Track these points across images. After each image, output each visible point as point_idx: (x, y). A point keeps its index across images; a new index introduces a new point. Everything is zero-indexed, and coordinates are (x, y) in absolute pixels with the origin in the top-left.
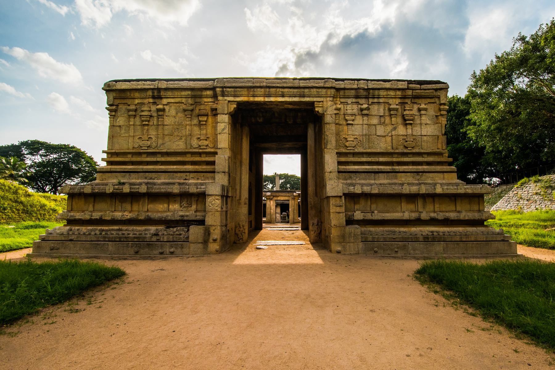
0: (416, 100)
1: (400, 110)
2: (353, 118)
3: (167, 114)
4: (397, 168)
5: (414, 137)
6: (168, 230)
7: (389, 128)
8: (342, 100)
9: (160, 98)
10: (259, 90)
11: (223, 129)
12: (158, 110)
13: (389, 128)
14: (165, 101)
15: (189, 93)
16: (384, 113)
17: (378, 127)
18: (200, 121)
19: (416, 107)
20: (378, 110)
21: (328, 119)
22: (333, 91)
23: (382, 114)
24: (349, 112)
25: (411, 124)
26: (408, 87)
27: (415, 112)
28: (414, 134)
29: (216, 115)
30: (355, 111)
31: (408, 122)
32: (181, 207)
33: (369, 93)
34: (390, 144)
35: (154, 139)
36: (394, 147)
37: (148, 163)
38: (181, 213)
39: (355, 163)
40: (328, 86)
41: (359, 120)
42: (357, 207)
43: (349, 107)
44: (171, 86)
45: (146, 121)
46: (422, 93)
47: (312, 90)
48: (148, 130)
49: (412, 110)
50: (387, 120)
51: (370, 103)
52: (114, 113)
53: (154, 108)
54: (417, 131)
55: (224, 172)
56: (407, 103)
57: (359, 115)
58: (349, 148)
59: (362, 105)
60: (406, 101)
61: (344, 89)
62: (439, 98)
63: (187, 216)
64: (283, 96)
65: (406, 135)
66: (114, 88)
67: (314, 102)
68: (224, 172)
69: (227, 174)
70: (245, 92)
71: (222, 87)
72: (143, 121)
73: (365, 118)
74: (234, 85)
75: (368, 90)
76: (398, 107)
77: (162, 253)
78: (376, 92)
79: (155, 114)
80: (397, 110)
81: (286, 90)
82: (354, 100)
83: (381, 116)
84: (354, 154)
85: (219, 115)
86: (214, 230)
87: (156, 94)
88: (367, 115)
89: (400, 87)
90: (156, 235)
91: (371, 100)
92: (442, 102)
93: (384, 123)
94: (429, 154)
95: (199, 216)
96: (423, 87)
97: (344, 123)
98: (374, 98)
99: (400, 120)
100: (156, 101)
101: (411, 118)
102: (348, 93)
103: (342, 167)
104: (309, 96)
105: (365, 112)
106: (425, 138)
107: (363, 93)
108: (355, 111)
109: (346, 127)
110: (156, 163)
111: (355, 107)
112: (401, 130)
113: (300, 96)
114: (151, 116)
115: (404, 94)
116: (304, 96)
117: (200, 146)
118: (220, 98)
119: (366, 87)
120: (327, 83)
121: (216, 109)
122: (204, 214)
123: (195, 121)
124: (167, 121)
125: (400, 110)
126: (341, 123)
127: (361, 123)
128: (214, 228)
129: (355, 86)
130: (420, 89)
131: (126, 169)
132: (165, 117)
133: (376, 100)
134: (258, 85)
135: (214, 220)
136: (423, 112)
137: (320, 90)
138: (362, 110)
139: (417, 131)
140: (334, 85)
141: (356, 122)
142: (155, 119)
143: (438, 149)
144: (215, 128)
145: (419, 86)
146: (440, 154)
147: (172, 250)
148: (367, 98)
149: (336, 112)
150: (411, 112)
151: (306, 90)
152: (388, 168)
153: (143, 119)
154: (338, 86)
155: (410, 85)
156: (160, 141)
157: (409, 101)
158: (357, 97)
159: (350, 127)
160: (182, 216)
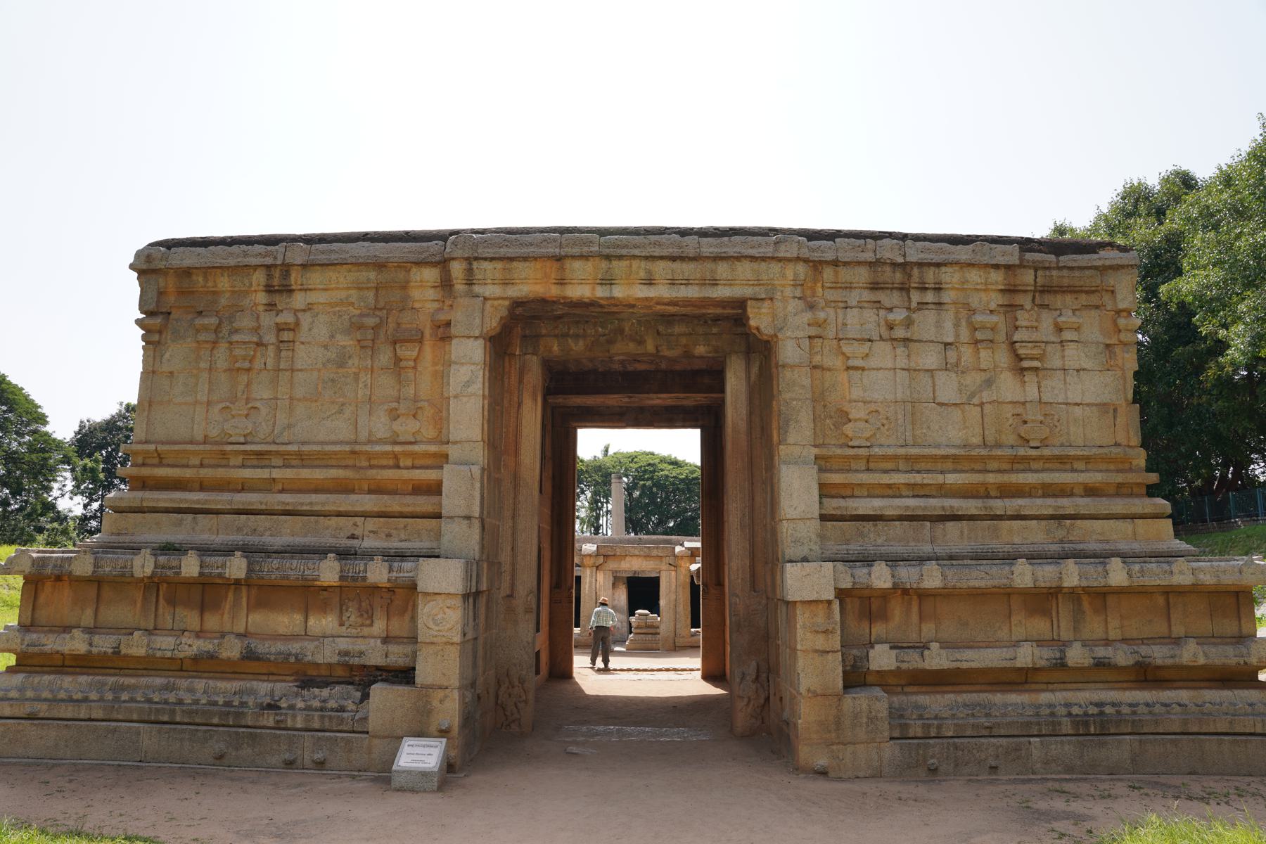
0: (1047, 299)
1: (1002, 327)
3: (303, 335)
4: (999, 506)
6: (305, 692)
8: (831, 295)
9: (288, 290)
10: (577, 264)
11: (468, 384)
12: (280, 328)
13: (973, 379)
15: (373, 275)
16: (957, 336)
17: (942, 377)
18: (398, 360)
19: (1047, 320)
20: (938, 325)
21: (789, 352)
22: (801, 268)
25: (1037, 369)
26: (1021, 259)
28: (1045, 399)
30: (872, 330)
32: (341, 625)
33: (910, 276)
34: (978, 430)
35: (264, 411)
37: (244, 487)
38: (343, 644)
39: (873, 491)
40: (788, 255)
41: (883, 355)
42: (879, 629)
43: (853, 317)
44: (322, 258)
46: (1066, 278)
48: (248, 385)
49: (1037, 326)
50: (967, 353)
51: (914, 305)
52: (156, 337)
53: (268, 320)
54: (1054, 389)
55: (468, 518)
56: (1021, 307)
57: (881, 339)
59: (890, 310)
61: (835, 263)
63: (361, 653)
64: (650, 282)
65: (1024, 403)
68: (468, 518)
69: (477, 524)
74: (503, 251)
75: (905, 266)
76: (995, 318)
77: (290, 764)
78: (930, 276)
79: (270, 338)
82: (867, 295)
83: (946, 344)
85: (454, 342)
86: (441, 701)
87: (276, 282)
88: (906, 341)
89: (1001, 260)
90: (273, 707)
91: (916, 297)
92: (1121, 306)
95: (396, 656)
96: (1066, 260)
97: (838, 363)
98: (924, 289)
99: (1003, 358)
100: (277, 298)
102: (845, 274)
104: (730, 283)
105: (900, 333)
106: (1078, 410)
108: (872, 330)
109: (843, 377)
110: (267, 486)
111: (870, 315)
112: (1008, 388)
113: (703, 283)
114: (259, 344)
116: (714, 283)
119: (901, 260)
120: (783, 248)
122: (409, 649)
123: (385, 357)
124: (305, 356)
126: (828, 362)
127: (890, 365)
128: (441, 694)
129: (869, 256)
131: (186, 501)
132: (298, 346)
133: (930, 297)
134: (576, 251)
135: (442, 668)
137: (764, 265)
139: (1054, 389)
140: (805, 253)
141: (873, 363)
142: (271, 351)
143: (1117, 445)
144: (441, 377)
145: (1052, 257)
146: (1122, 464)
147: (318, 756)
148: (904, 289)
149: (813, 331)
151: (722, 269)
152: (971, 506)
154: (816, 256)
156: (282, 419)
157: (1026, 300)
158: (875, 287)
159: (856, 375)
160: (347, 654)
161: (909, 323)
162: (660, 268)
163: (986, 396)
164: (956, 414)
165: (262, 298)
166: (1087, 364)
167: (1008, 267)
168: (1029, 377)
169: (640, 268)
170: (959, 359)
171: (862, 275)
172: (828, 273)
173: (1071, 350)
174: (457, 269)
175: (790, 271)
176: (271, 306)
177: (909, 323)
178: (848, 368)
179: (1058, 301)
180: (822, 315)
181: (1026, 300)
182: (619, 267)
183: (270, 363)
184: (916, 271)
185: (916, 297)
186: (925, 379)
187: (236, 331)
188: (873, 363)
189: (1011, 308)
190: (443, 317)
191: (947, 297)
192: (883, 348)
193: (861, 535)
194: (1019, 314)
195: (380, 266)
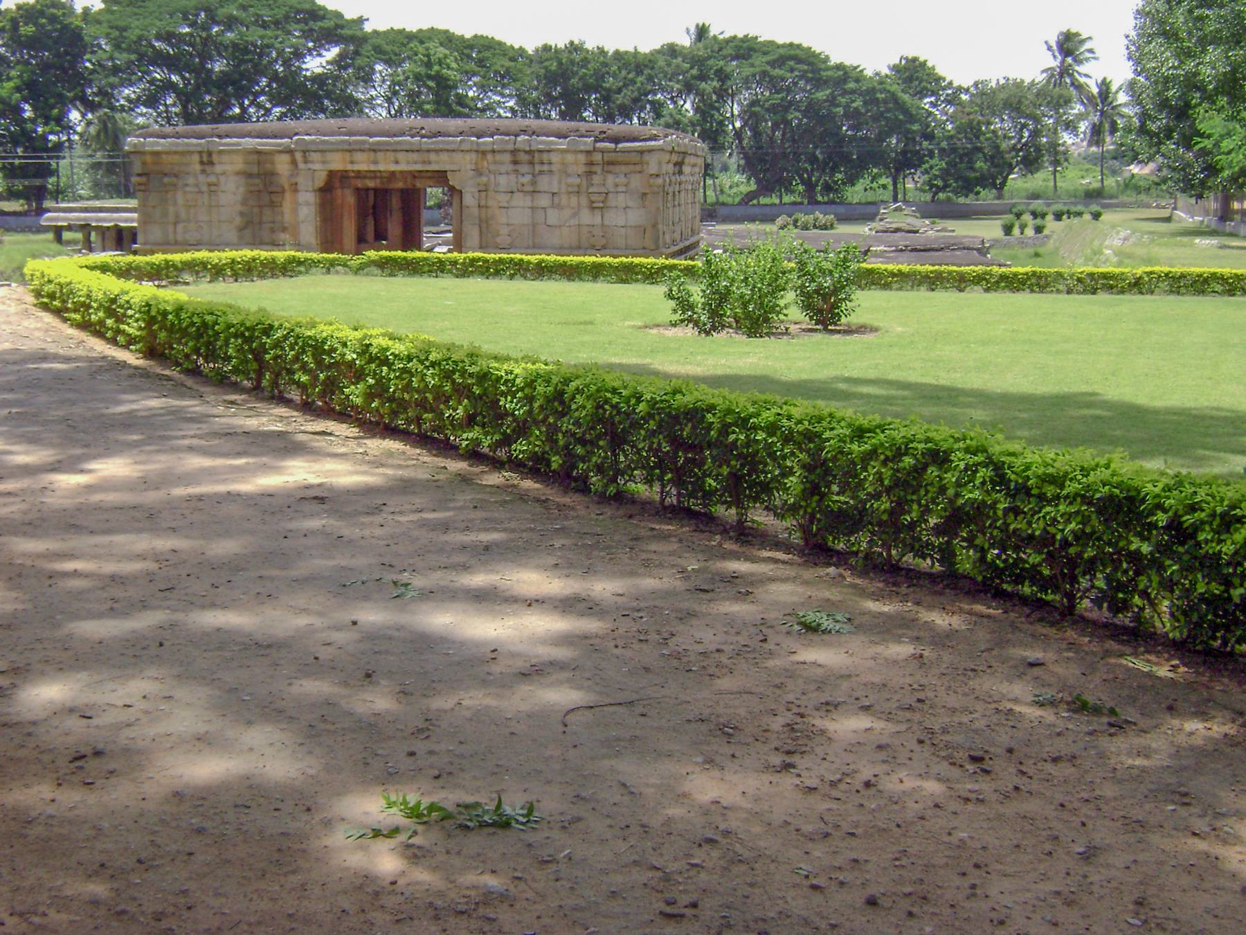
0: (611, 168)
1: (584, 182)
3: (223, 188)
7: (567, 213)
12: (209, 185)
13: (567, 213)
19: (610, 179)
22: (474, 156)
29: (296, 191)
41: (520, 201)
46: (620, 157)
53: (202, 178)
60: (595, 168)
64: (397, 162)
71: (304, 152)
74: (321, 147)
75: (530, 152)
78: (545, 157)
79: (205, 188)
82: (511, 167)
87: (205, 159)
91: (538, 168)
99: (584, 201)
102: (498, 157)
104: (437, 163)
107: (524, 157)
111: (513, 177)
112: (586, 217)
113: (424, 162)
114: (201, 192)
116: (430, 163)
129: (511, 147)
130: (615, 151)
133: (545, 168)
134: (357, 147)
140: (475, 148)
141: (513, 203)
142: (206, 195)
144: (295, 211)
145: (612, 146)
148: (531, 163)
150: (603, 190)
151: (433, 157)
154: (482, 148)
155: (598, 145)
157: (598, 169)
161: (534, 183)
162: (401, 156)
163: (574, 222)
165: (198, 167)
166: (630, 204)
167: (588, 152)
169: (391, 155)
171: (507, 158)
172: (489, 157)
173: (621, 197)
174: (298, 156)
175: (468, 157)
176: (203, 171)
177: (534, 183)
179: (617, 169)
180: (484, 179)
181: (598, 169)
182: (380, 155)
183: (206, 202)
184: (536, 155)
185: (538, 168)
186: (541, 212)
187: (186, 185)
188: (513, 203)
189: (590, 174)
190: (294, 180)
191: (554, 168)
195: (259, 152)
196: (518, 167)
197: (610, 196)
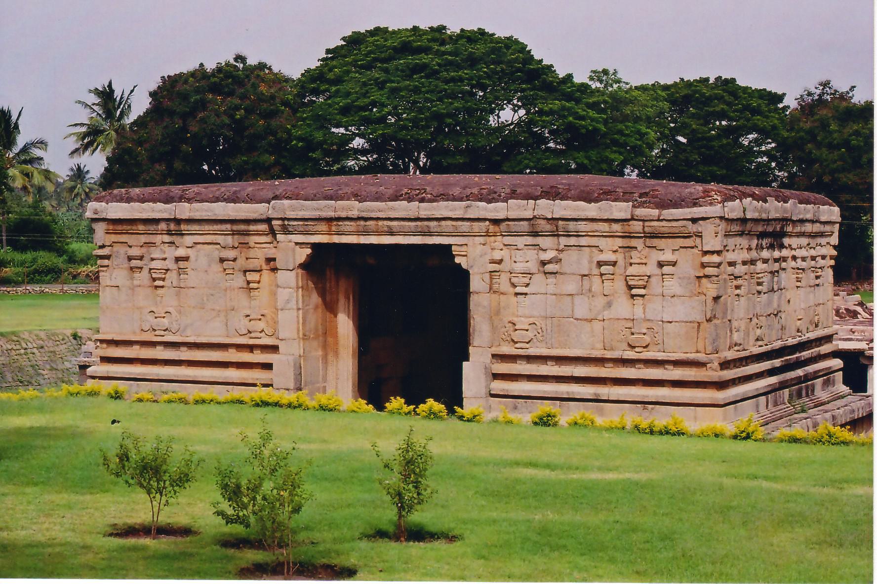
0: (655, 242)
1: (621, 262)
2: (526, 280)
4: (605, 391)
5: (649, 325)
7: (601, 301)
8: (508, 240)
11: (288, 301)
12: (178, 259)
14: (189, 240)
15: (228, 226)
18: (248, 283)
21: (476, 283)
23: (586, 273)
24: (519, 267)
25: (643, 296)
26: (632, 216)
27: (651, 268)
28: (648, 317)
31: (634, 291)
36: (608, 346)
39: (531, 378)
41: (539, 283)
44: (197, 215)
45: (160, 279)
47: (443, 223)
49: (646, 260)
50: (597, 280)
54: (655, 309)
55: (288, 390)
58: (517, 345)
62: (699, 235)
64: (391, 233)
66: (103, 216)
67: (450, 246)
68: (288, 390)
70: (323, 227)
71: (283, 219)
72: (154, 280)
73: (551, 280)
78: (572, 226)
80: (614, 264)
81: (395, 223)
84: (530, 359)
91: (563, 241)
93: (590, 290)
94: (677, 363)
97: (512, 290)
99: (620, 285)
101: (641, 283)
103: (499, 386)
104: (440, 234)
105: (550, 268)
108: (533, 266)
109: (514, 299)
111: (532, 254)
112: (623, 307)
115: (627, 228)
117: (250, 332)
118: (280, 237)
119: (550, 217)
120: (469, 210)
121: (274, 259)
123: (239, 281)
125: (621, 262)
129: (528, 214)
133: (573, 241)
136: (666, 269)
137: (460, 223)
138: (543, 263)
139: (655, 309)
143: (697, 352)
145: (655, 212)
150: (641, 270)
151: (433, 224)
153: (154, 275)
155: (641, 212)
157: (638, 243)
158: (535, 234)
164: (587, 325)
168: (639, 301)
170: (591, 287)
178: (517, 294)
192: (539, 278)
193: (515, 408)
194: (634, 253)
196: (539, 240)
197: (653, 280)
